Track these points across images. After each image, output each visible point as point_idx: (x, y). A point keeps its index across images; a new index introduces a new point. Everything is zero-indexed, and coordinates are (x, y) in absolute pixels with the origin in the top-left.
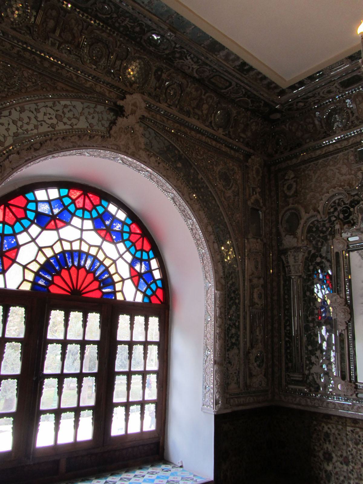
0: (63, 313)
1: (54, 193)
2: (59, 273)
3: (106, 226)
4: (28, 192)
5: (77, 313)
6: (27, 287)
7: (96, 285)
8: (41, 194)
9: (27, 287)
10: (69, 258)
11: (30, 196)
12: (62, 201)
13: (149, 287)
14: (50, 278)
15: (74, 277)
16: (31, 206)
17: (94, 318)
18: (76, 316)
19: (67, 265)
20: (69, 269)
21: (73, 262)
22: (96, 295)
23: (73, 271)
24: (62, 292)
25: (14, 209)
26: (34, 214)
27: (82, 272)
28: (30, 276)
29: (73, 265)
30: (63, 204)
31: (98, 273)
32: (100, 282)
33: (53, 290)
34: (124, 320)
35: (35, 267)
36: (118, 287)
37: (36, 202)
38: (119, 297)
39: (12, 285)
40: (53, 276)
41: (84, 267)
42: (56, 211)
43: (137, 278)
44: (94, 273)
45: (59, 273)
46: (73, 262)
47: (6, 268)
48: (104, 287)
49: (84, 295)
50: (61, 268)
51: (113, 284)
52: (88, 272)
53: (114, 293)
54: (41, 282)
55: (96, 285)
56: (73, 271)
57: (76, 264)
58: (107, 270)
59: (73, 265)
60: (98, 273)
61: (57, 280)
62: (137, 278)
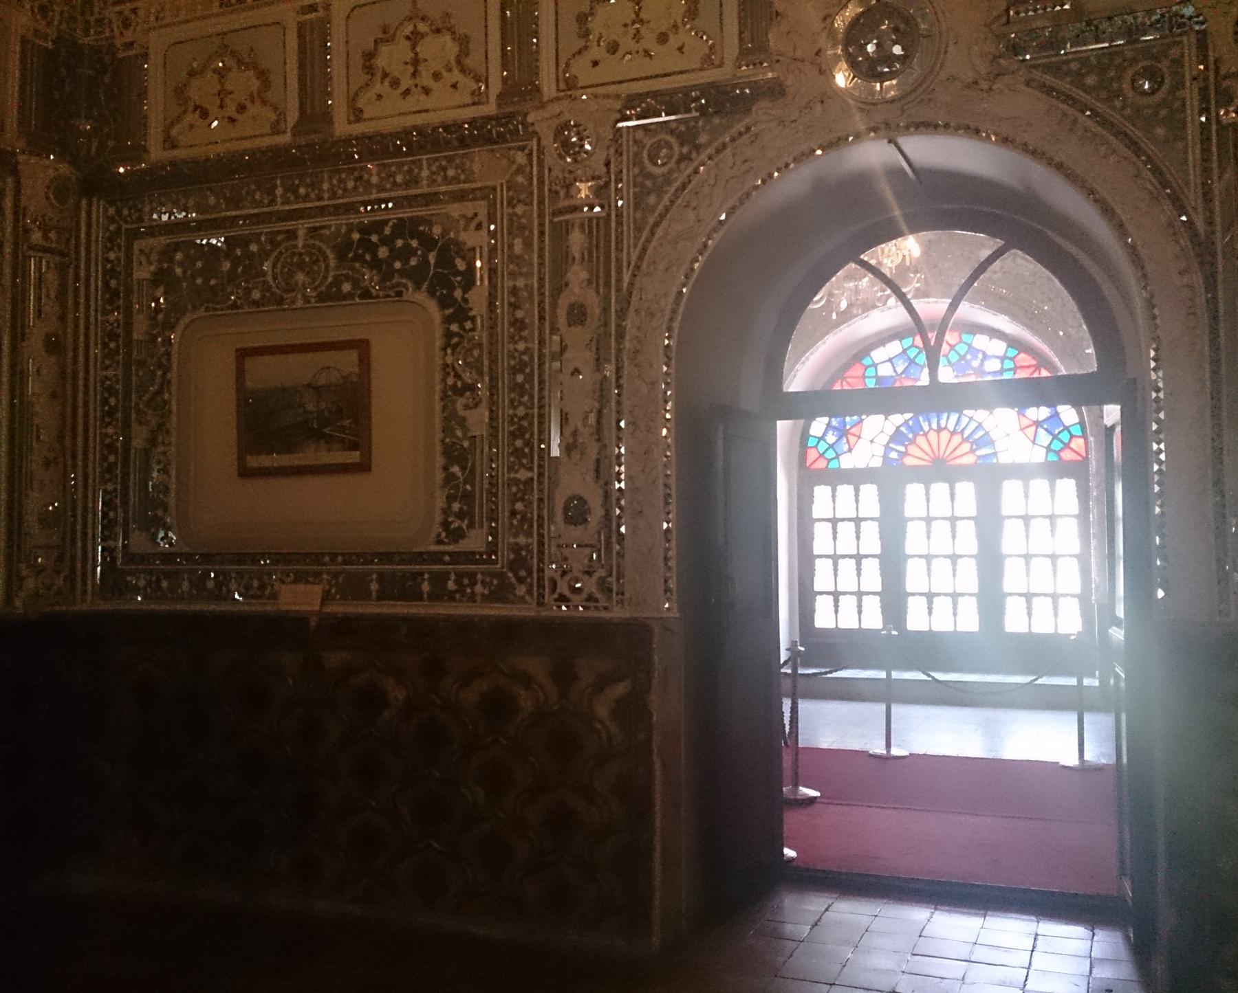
0: (852, 487)
1: (894, 348)
2: (913, 442)
3: (973, 369)
4: (863, 358)
5: (869, 486)
6: (877, 463)
7: (966, 447)
8: (878, 355)
9: (877, 463)
10: (924, 421)
11: (867, 361)
12: (906, 354)
13: (1055, 437)
14: (902, 449)
15: (934, 444)
16: (870, 372)
17: (966, 491)
18: (940, 490)
19: (922, 429)
20: (926, 434)
21: (930, 425)
22: (970, 459)
23: (932, 436)
24: (927, 463)
25: (849, 380)
26: (874, 380)
27: (945, 435)
28: (880, 451)
29: (931, 428)
30: (909, 358)
31: (966, 434)
32: (972, 443)
33: (909, 461)
34: (1011, 491)
35: (884, 439)
36: (999, 446)
37: (875, 365)
38: (1004, 459)
39: (861, 464)
40: (906, 447)
41: (946, 428)
42: (900, 370)
43: (1033, 428)
44: (962, 432)
45: (913, 442)
46: (930, 425)
47: (852, 445)
48: (979, 448)
49: (952, 463)
50: (915, 436)
51: (991, 443)
52: (953, 433)
53: (995, 454)
54: (894, 455)
55: (966, 447)
56: (932, 436)
57: (934, 426)
58: (980, 426)
59: (931, 428)
60: (966, 434)
61: (913, 450)
62: (1031, 430)
